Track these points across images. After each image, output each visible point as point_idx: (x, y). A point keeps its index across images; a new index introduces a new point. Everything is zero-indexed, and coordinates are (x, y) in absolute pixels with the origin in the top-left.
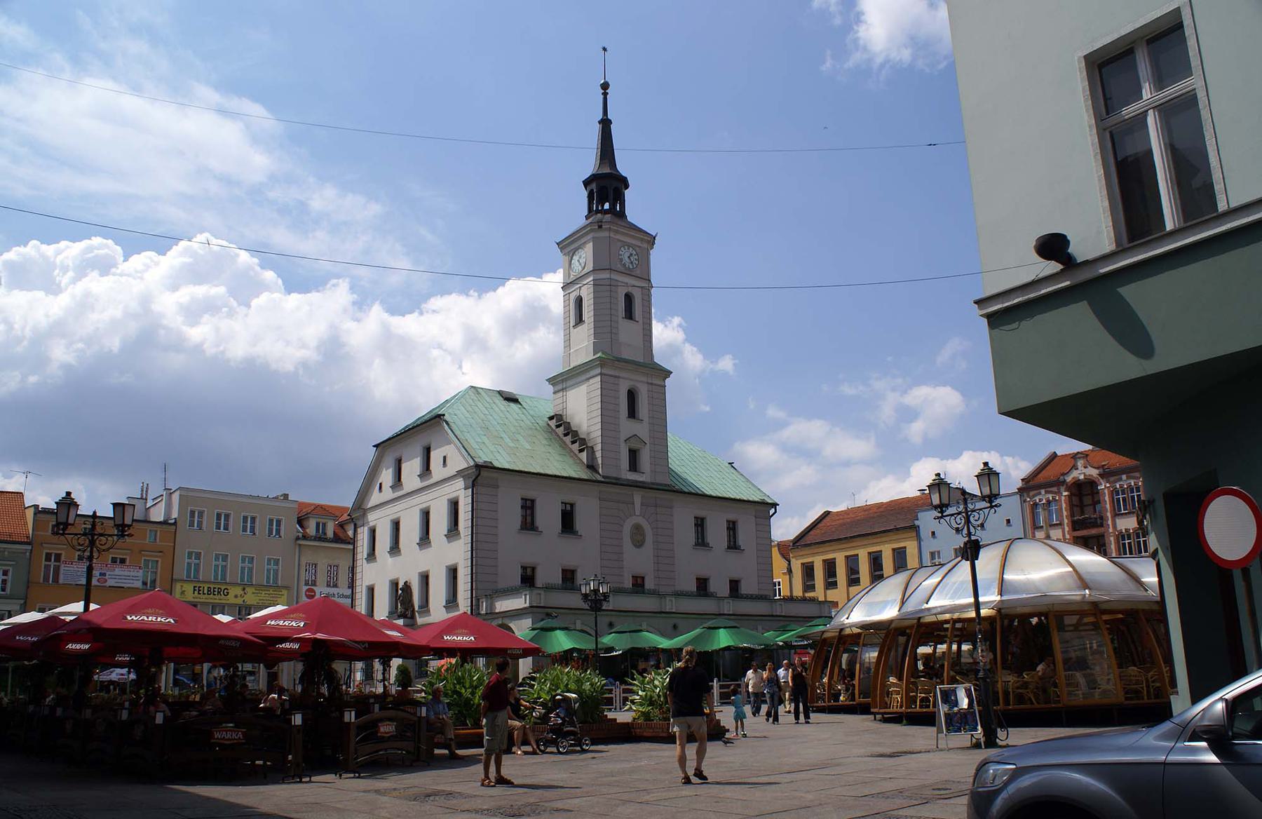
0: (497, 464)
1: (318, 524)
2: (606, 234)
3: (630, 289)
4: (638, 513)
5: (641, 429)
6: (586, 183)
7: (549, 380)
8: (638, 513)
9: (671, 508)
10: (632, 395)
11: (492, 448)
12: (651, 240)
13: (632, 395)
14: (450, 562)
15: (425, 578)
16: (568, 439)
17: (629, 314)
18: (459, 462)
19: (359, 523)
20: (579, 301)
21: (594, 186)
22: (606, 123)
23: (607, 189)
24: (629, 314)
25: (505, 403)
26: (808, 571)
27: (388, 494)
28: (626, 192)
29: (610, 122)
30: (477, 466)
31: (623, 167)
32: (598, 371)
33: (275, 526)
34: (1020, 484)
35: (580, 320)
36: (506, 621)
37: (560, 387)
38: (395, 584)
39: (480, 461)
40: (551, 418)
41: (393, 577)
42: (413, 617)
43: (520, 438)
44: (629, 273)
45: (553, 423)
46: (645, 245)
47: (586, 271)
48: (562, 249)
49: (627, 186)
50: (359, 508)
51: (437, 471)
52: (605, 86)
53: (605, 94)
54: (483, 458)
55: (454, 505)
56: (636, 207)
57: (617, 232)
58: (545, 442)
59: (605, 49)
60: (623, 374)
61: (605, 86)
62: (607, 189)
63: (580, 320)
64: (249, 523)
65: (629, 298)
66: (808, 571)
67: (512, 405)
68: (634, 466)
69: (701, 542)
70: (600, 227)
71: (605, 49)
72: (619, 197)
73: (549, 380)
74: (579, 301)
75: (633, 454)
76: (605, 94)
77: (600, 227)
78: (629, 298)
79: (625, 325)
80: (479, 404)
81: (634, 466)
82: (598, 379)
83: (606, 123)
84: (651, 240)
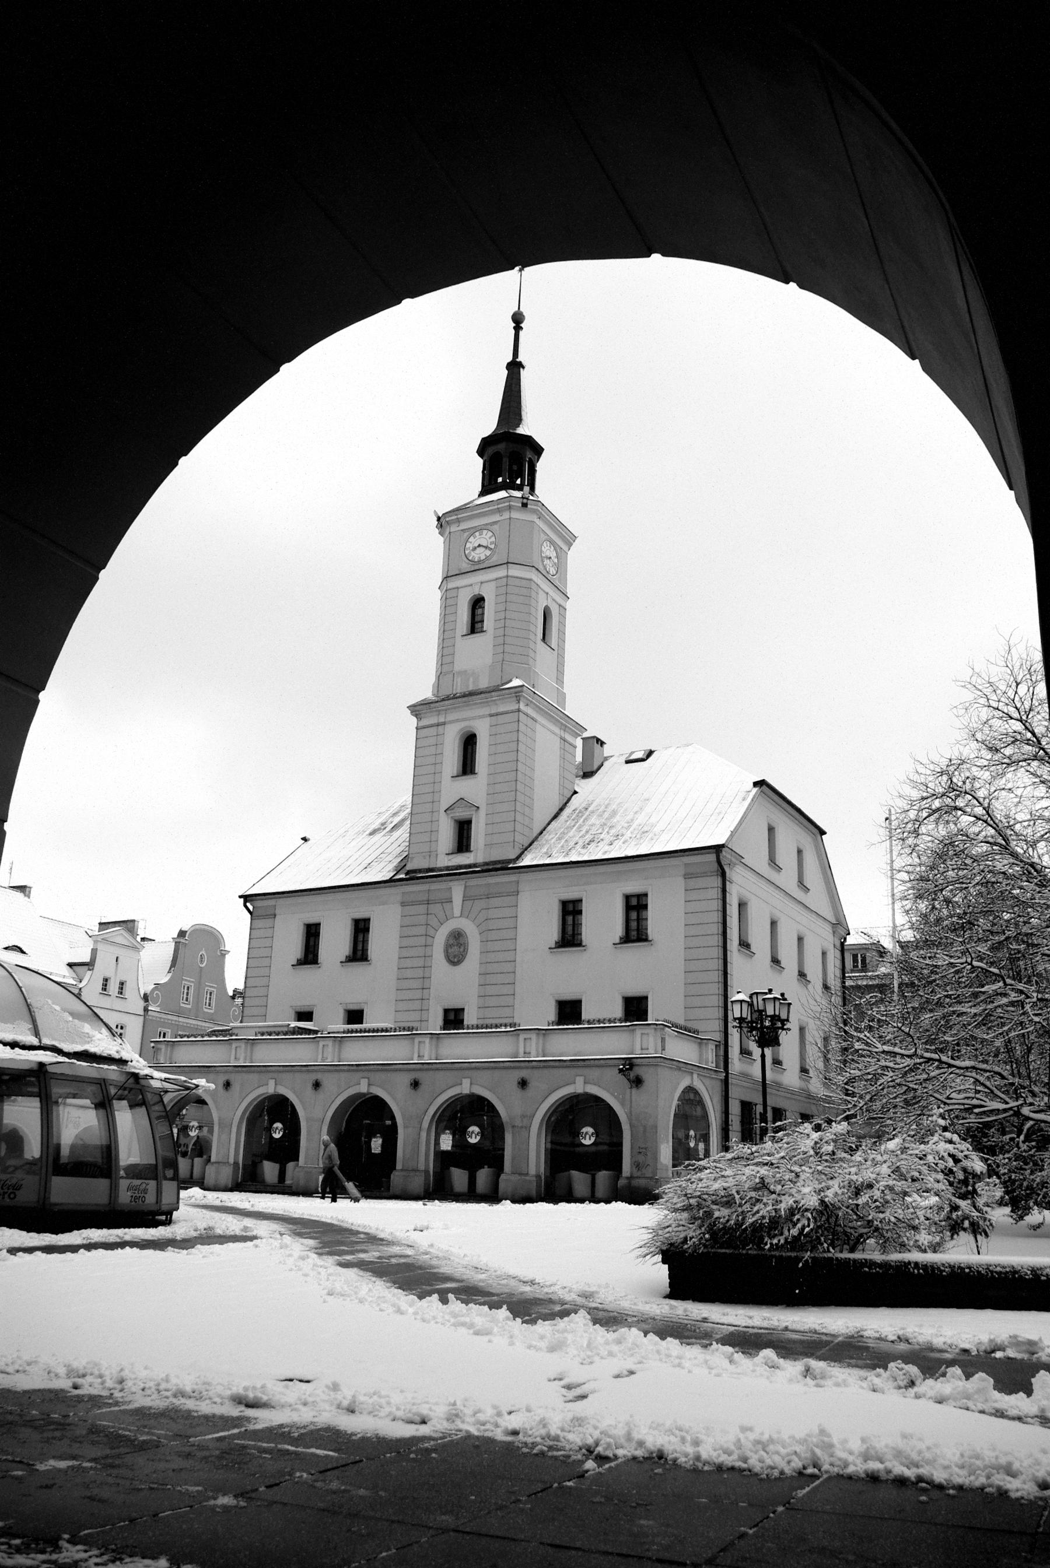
20: (478, 603)
21: (501, 447)
22: (515, 367)
23: (509, 457)
35: (475, 626)
46: (565, 548)
47: (494, 560)
52: (518, 320)
53: (518, 328)
61: (518, 320)
62: (509, 457)
63: (475, 626)
65: (547, 615)
74: (478, 603)
76: (518, 328)
78: (547, 615)
83: (515, 367)
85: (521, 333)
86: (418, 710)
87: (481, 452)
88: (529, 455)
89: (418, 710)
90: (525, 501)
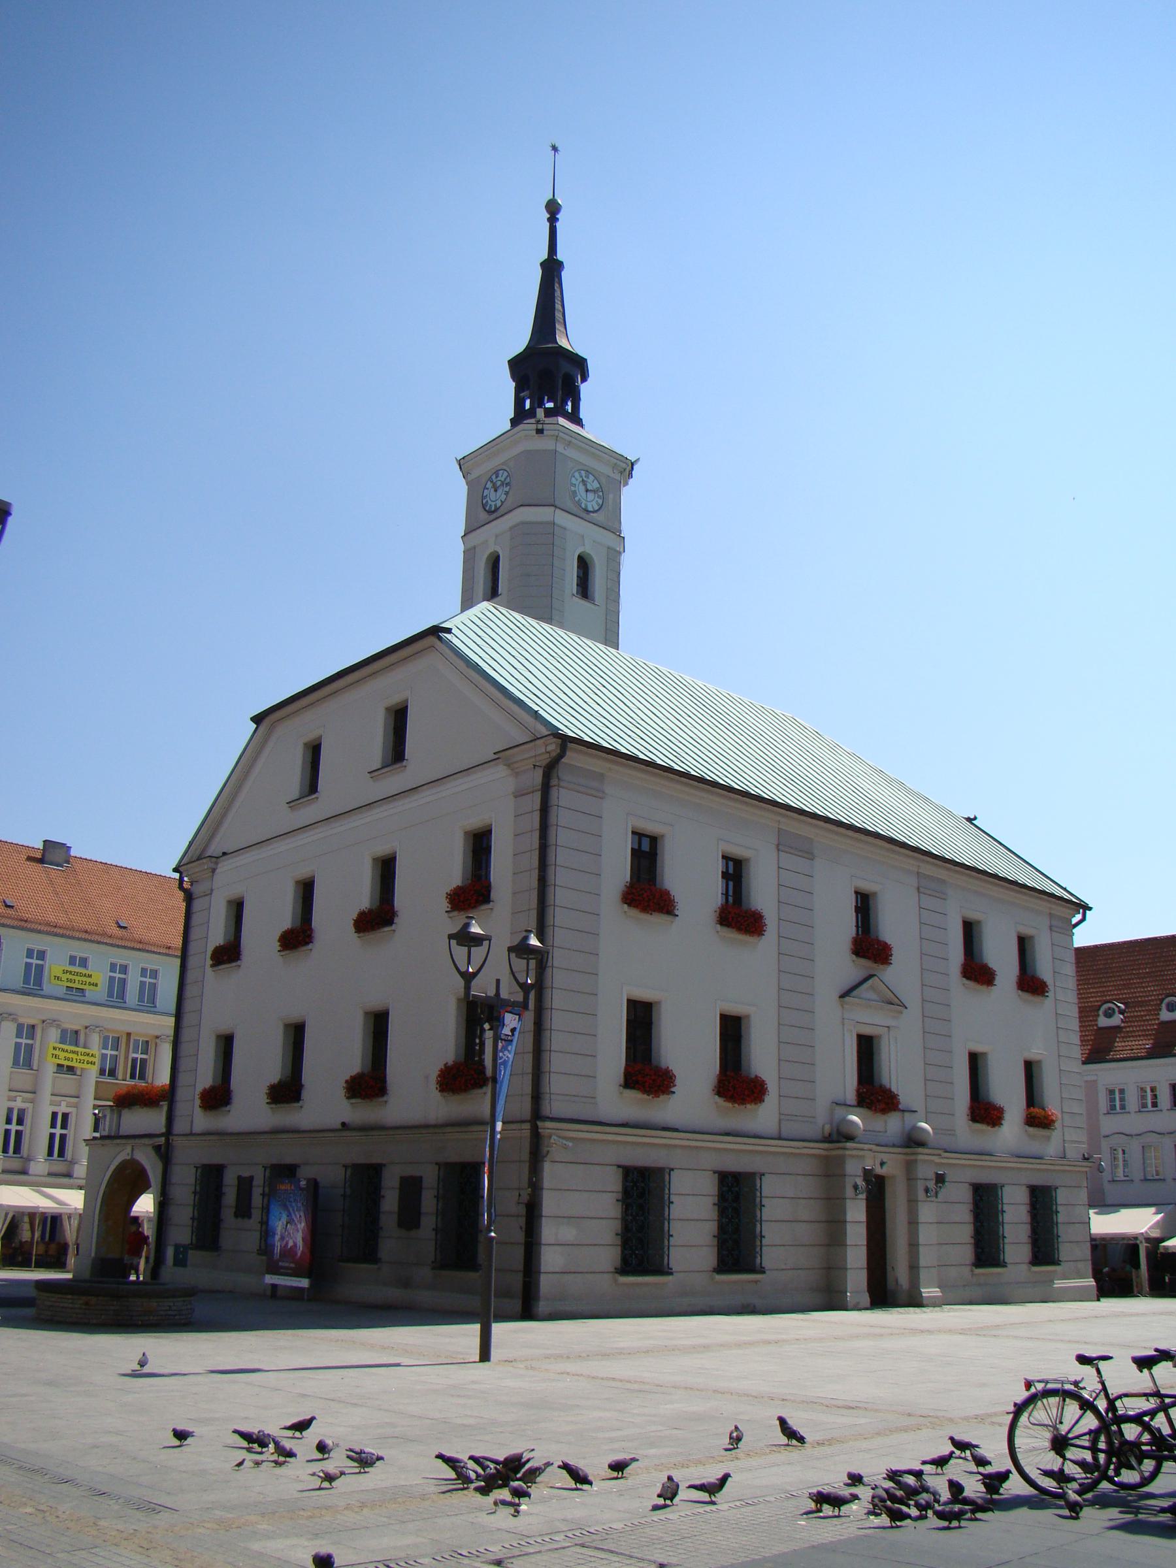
3: (588, 549)
6: (516, 365)
20: (494, 563)
22: (552, 269)
23: (548, 375)
29: (559, 265)
44: (584, 513)
52: (553, 209)
53: (553, 220)
59: (555, 149)
61: (553, 209)
62: (548, 375)
65: (584, 564)
71: (555, 149)
74: (494, 563)
76: (553, 220)
78: (584, 564)
83: (552, 269)
85: (558, 225)
87: (514, 376)
88: (566, 367)
90: (540, 427)
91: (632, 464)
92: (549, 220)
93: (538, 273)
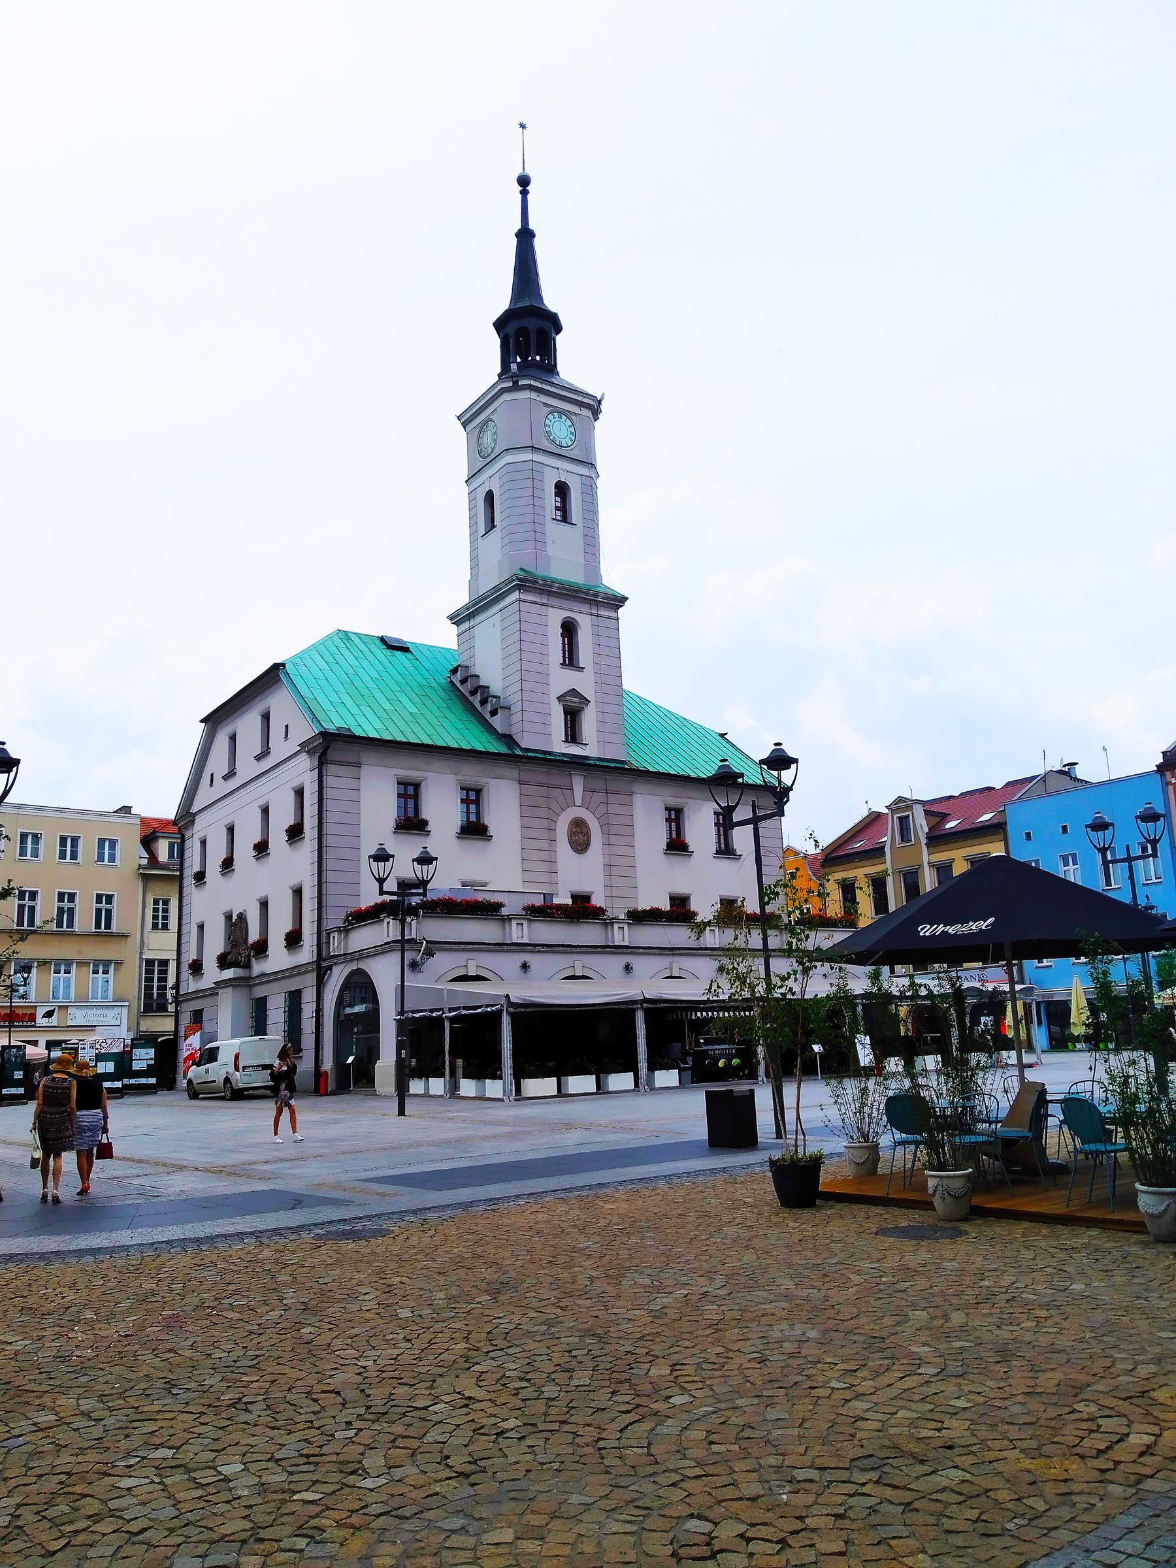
0: (358, 732)
1: (171, 845)
2: (526, 394)
4: (578, 802)
5: (584, 683)
7: (451, 618)
8: (578, 802)
9: (631, 794)
10: (569, 630)
11: (354, 710)
12: (594, 407)
13: (569, 630)
14: (294, 881)
15: (264, 905)
16: (476, 700)
17: (564, 514)
18: (304, 731)
19: (188, 834)
20: (490, 497)
22: (525, 236)
23: (528, 334)
24: (564, 514)
25: (387, 652)
26: (848, 889)
27: (222, 787)
28: (559, 338)
29: (532, 234)
30: (325, 735)
31: (552, 300)
32: (515, 595)
33: (106, 846)
34: (1160, 759)
35: (491, 525)
36: (363, 965)
37: (466, 625)
38: (228, 916)
39: (331, 728)
40: (454, 671)
41: (226, 909)
42: (247, 966)
43: (404, 699)
45: (456, 679)
46: (588, 413)
48: (464, 425)
49: (558, 329)
50: (188, 812)
51: (280, 748)
52: (524, 182)
53: (524, 193)
54: (335, 722)
55: (299, 793)
56: (573, 361)
57: (540, 391)
58: (441, 704)
59: (523, 126)
60: (553, 601)
61: (524, 182)
62: (528, 334)
63: (491, 525)
64: (68, 845)
65: (562, 490)
66: (848, 889)
67: (399, 654)
68: (573, 734)
69: (677, 846)
70: (516, 383)
71: (523, 126)
72: (547, 348)
73: (451, 618)
74: (490, 497)
75: (573, 716)
76: (524, 193)
77: (516, 383)
78: (562, 490)
79: (555, 531)
80: (346, 652)
81: (573, 734)
82: (516, 606)
83: (525, 236)
84: (594, 407)
86: (457, 619)
89: (457, 619)
91: (599, 402)
92: (521, 192)
93: (514, 241)
